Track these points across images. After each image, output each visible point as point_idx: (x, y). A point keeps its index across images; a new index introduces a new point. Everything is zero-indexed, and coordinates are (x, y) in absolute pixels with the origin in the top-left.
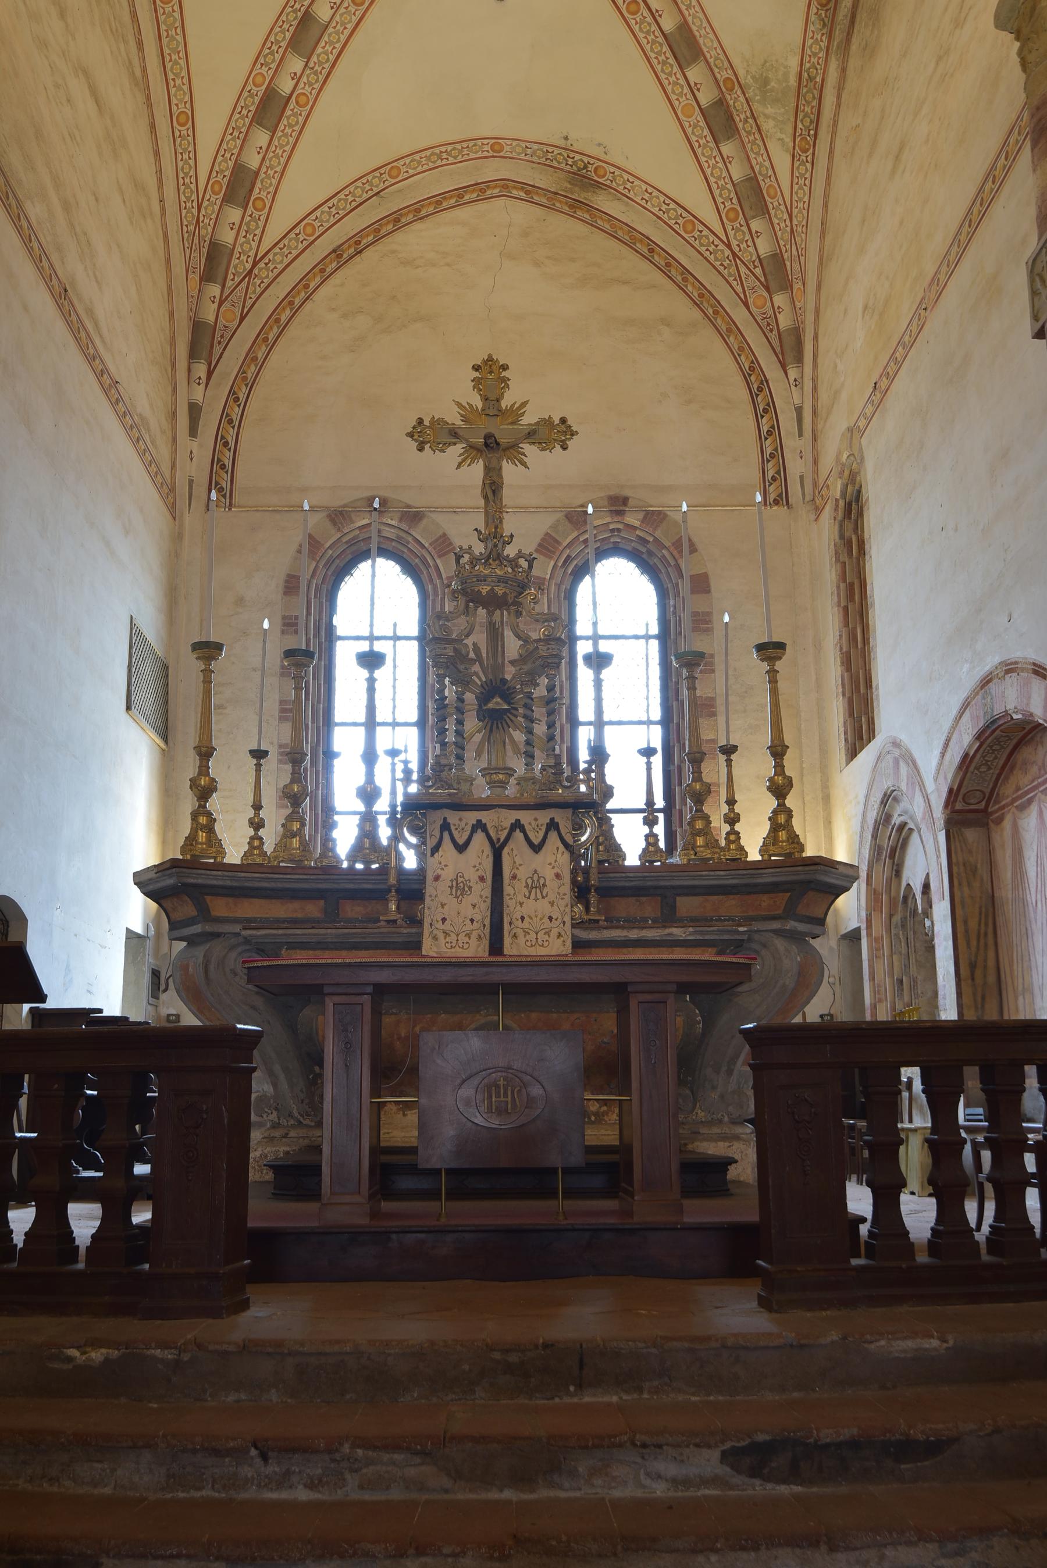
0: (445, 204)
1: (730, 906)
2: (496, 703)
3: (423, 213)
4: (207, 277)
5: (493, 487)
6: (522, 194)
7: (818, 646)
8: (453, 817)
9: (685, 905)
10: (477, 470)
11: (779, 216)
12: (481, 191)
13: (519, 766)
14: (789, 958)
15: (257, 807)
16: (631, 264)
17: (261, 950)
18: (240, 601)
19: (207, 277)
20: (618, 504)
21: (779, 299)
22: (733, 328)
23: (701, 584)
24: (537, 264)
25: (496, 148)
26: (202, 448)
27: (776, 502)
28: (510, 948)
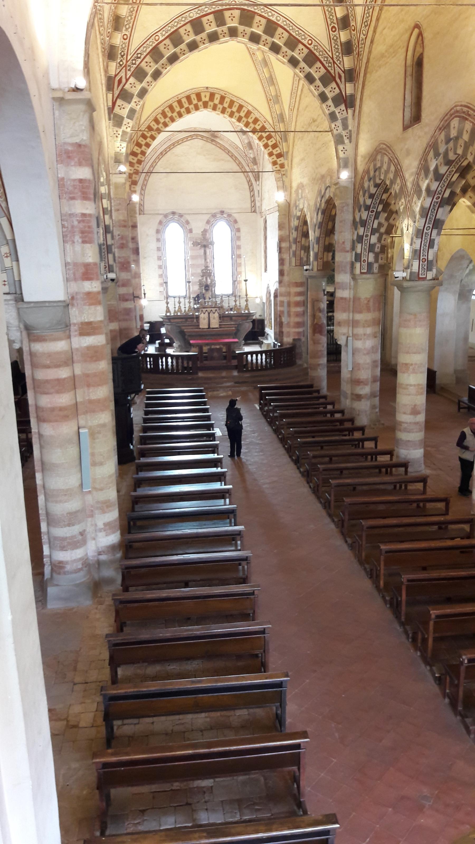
0: (184, 141)
1: (240, 318)
2: (207, 288)
3: (180, 143)
5: (205, 253)
6: (201, 138)
7: (261, 245)
8: (203, 309)
9: (233, 318)
10: (202, 251)
11: (255, 150)
15: (175, 305)
16: (225, 156)
17: (179, 327)
18: (147, 235)
20: (222, 212)
21: (255, 167)
23: (238, 230)
24: (205, 156)
27: (254, 212)
28: (211, 326)
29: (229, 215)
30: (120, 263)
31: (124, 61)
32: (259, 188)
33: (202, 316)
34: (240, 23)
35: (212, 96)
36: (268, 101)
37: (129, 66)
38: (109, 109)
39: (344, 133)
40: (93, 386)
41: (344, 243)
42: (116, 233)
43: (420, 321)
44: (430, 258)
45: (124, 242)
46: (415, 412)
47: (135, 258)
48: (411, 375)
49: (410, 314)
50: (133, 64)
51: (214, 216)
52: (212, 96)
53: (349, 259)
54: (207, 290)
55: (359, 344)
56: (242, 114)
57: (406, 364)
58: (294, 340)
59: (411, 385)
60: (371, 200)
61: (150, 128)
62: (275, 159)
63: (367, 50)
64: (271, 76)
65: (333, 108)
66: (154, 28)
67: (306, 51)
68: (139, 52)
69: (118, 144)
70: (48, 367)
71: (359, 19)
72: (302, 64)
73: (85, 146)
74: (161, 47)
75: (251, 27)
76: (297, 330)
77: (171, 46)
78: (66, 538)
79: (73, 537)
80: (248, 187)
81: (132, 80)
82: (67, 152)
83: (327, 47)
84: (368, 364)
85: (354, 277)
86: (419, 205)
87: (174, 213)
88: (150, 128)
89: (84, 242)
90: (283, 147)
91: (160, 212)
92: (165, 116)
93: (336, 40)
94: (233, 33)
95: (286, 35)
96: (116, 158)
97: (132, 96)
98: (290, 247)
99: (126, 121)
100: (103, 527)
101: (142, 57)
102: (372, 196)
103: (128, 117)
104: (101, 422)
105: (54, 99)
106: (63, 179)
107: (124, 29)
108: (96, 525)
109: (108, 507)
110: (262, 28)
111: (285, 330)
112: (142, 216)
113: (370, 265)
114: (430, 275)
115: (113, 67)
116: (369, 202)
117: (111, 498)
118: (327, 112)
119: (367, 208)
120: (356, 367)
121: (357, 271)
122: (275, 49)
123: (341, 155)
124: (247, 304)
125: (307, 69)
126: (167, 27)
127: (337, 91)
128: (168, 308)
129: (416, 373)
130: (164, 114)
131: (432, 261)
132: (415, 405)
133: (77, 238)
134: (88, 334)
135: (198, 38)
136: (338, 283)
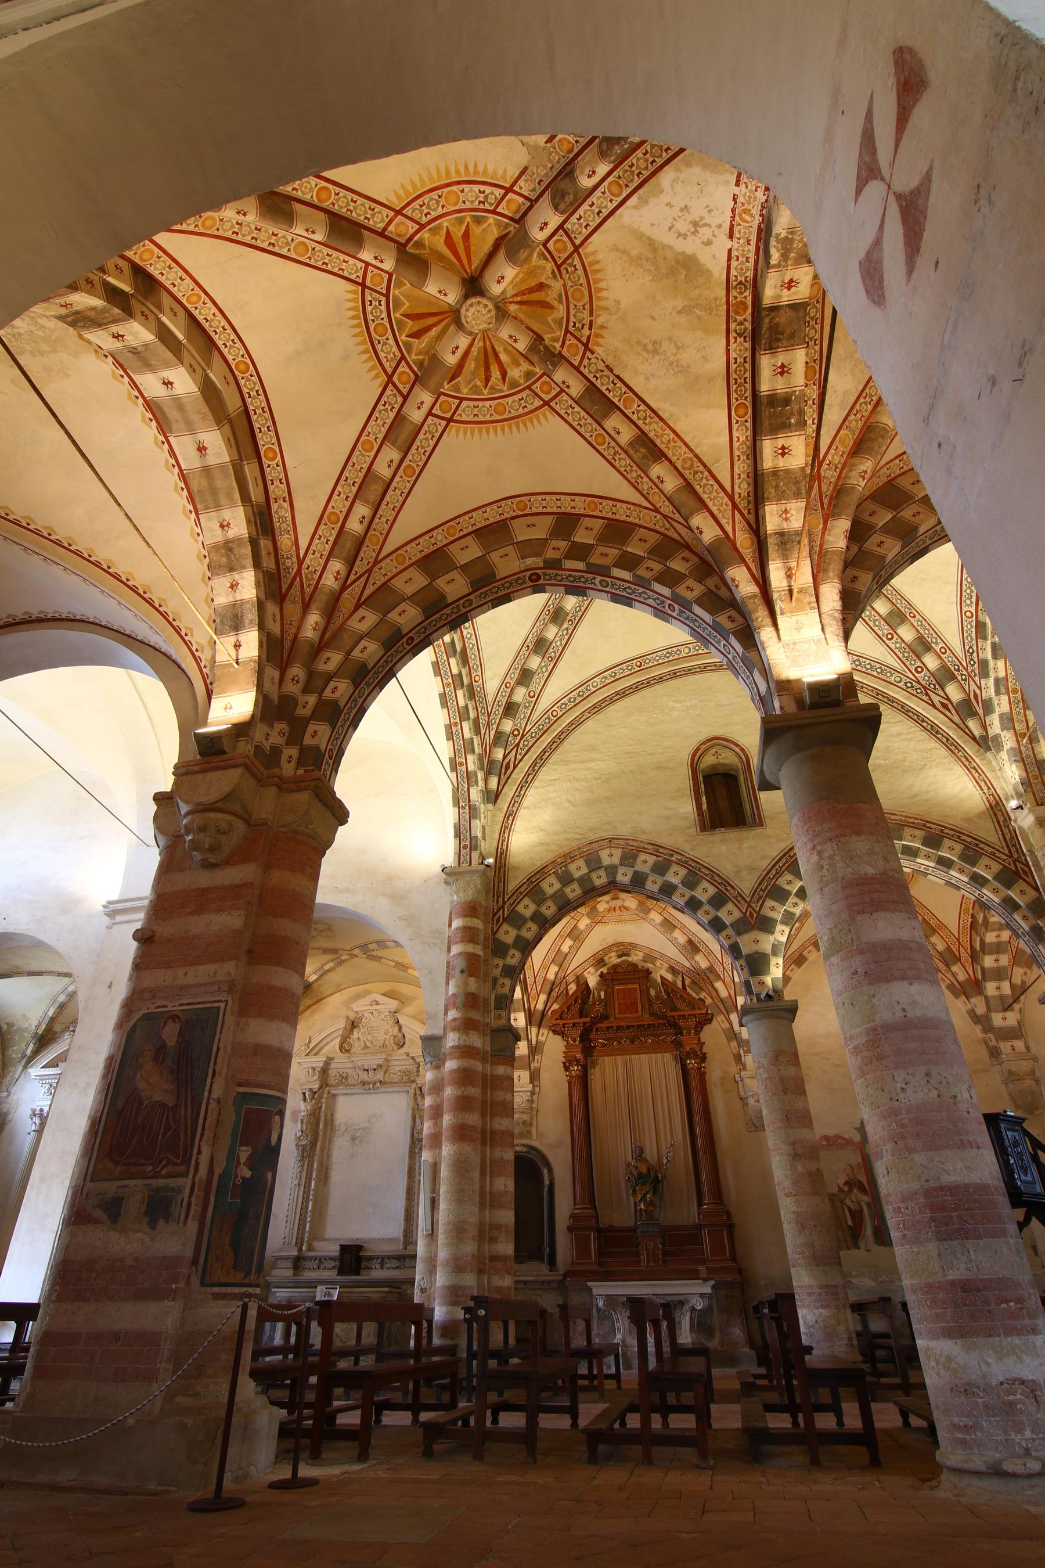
31: (965, 672)
37: (973, 671)
50: (973, 665)
66: (952, 612)
68: (967, 647)
81: (983, 682)
101: (974, 648)
107: (934, 645)
126: (964, 594)
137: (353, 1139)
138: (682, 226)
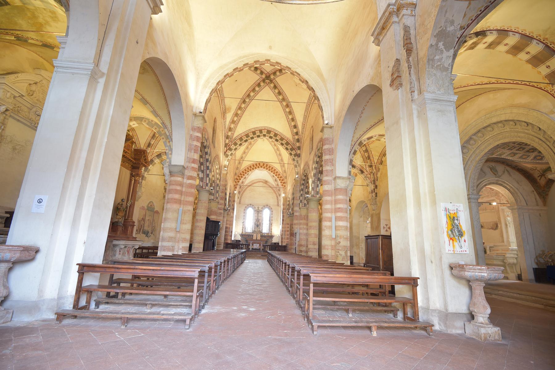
1: (268, 237)
4: (240, 188)
10: (257, 213)
12: (259, 182)
13: (258, 229)
14: (271, 240)
17: (246, 238)
18: (241, 211)
19: (240, 188)
20: (267, 205)
22: (276, 193)
23: (272, 211)
25: (260, 179)
26: (239, 200)
29: (269, 206)
30: (220, 197)
32: (280, 199)
33: (254, 235)
34: (267, 133)
35: (264, 164)
36: (281, 166)
38: (224, 152)
39: (297, 164)
40: (188, 196)
41: (297, 197)
42: (221, 188)
43: (315, 211)
44: (318, 190)
45: (223, 191)
46: (314, 244)
47: (233, 211)
48: (313, 230)
49: (311, 208)
51: (264, 206)
52: (264, 164)
53: (298, 203)
54: (257, 227)
55: (301, 231)
56: (273, 170)
57: (311, 226)
58: (286, 244)
59: (312, 234)
60: (304, 182)
61: (243, 172)
62: (283, 184)
63: (303, 140)
64: (282, 159)
65: (294, 157)
67: (286, 141)
69: (226, 162)
70: (173, 185)
71: (301, 132)
72: (285, 145)
73: (201, 128)
74: (243, 138)
75: (270, 134)
76: (287, 240)
77: (246, 137)
78: (166, 246)
79: (169, 246)
80: (276, 198)
81: (233, 145)
82: (195, 128)
83: (292, 140)
84: (305, 239)
85: (300, 208)
86: (313, 173)
87: (251, 204)
88: (243, 172)
89: (194, 152)
90: (285, 181)
91: (246, 204)
92: (248, 169)
93: (295, 139)
94: (264, 135)
95: (280, 137)
96: (225, 166)
97: (232, 149)
98: (286, 212)
99: (229, 156)
100: (181, 248)
102: (304, 180)
103: (230, 155)
104: (189, 209)
105: (193, 114)
106: (192, 134)
108: (179, 247)
109: (185, 240)
110: (273, 135)
111: (283, 240)
112: (240, 205)
113: (305, 204)
114: (318, 196)
115: (227, 141)
116: (303, 182)
117: (187, 238)
118: (292, 158)
119: (303, 184)
120: (300, 239)
121: (301, 206)
122: (277, 140)
123: (296, 171)
124: (271, 232)
125: (286, 146)
127: (295, 153)
128: (242, 232)
129: (314, 229)
130: (248, 168)
131: (318, 192)
132: (314, 242)
133: (193, 151)
134: (190, 179)
135: (254, 136)
136: (295, 210)
137: (14, 149)
138: (356, 158)
